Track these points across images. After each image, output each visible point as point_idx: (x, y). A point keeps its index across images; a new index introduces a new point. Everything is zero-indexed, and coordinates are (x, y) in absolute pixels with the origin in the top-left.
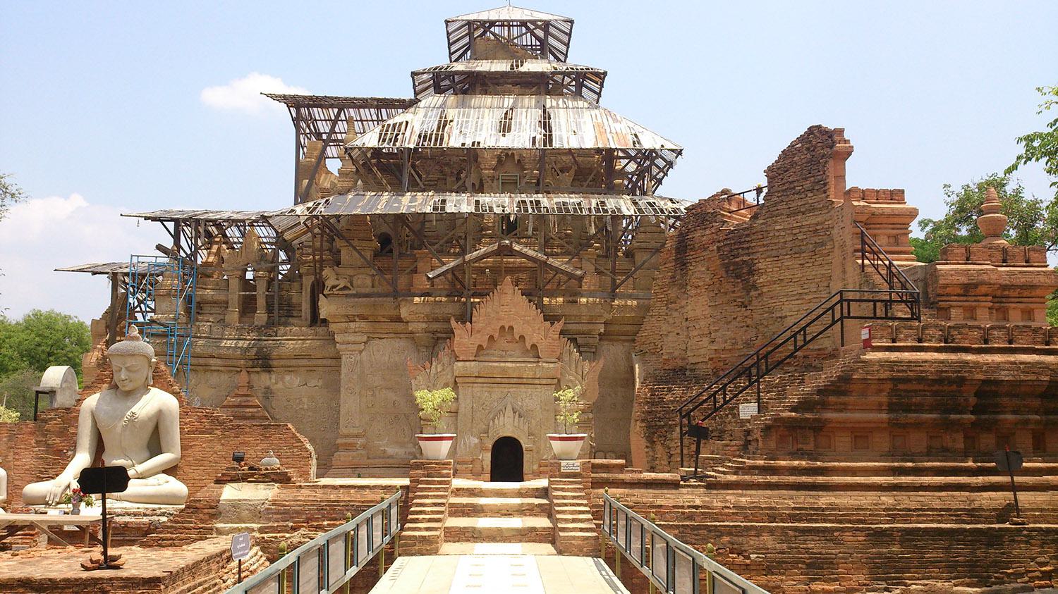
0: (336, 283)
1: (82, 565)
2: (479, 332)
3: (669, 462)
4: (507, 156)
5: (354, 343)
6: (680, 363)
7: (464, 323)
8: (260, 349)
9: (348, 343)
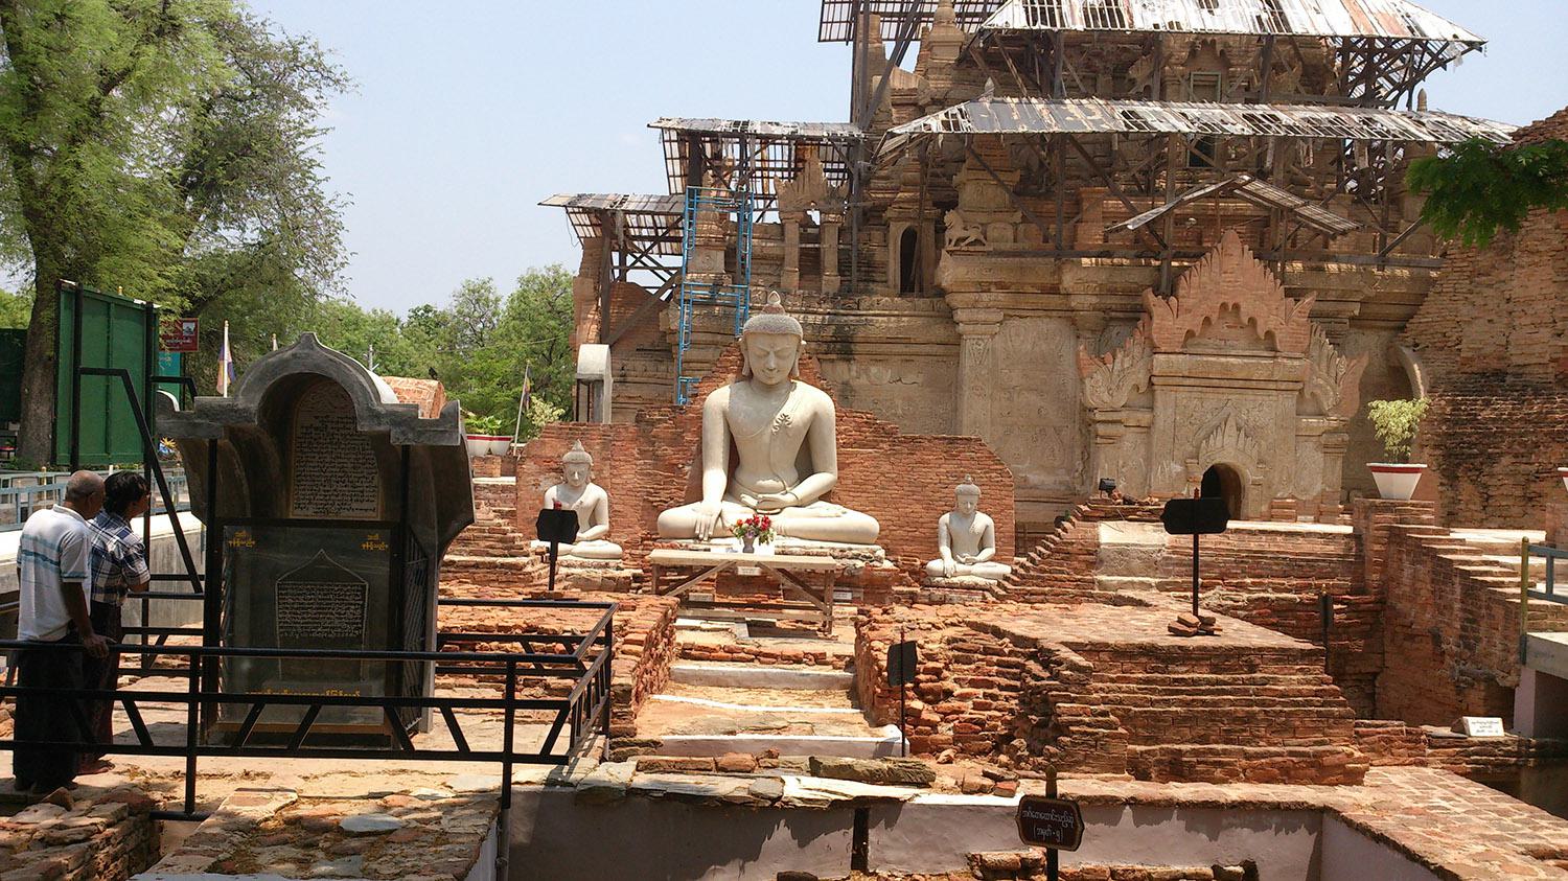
0: (963, 234)
1: (1170, 629)
2: (1188, 311)
3: (1485, 507)
4: (1205, 44)
5: (985, 323)
6: (1495, 365)
7: (1166, 297)
8: (840, 327)
9: (976, 323)
